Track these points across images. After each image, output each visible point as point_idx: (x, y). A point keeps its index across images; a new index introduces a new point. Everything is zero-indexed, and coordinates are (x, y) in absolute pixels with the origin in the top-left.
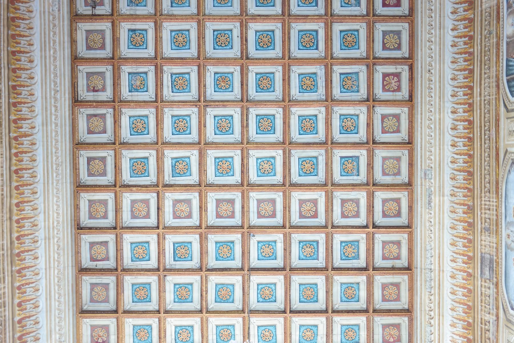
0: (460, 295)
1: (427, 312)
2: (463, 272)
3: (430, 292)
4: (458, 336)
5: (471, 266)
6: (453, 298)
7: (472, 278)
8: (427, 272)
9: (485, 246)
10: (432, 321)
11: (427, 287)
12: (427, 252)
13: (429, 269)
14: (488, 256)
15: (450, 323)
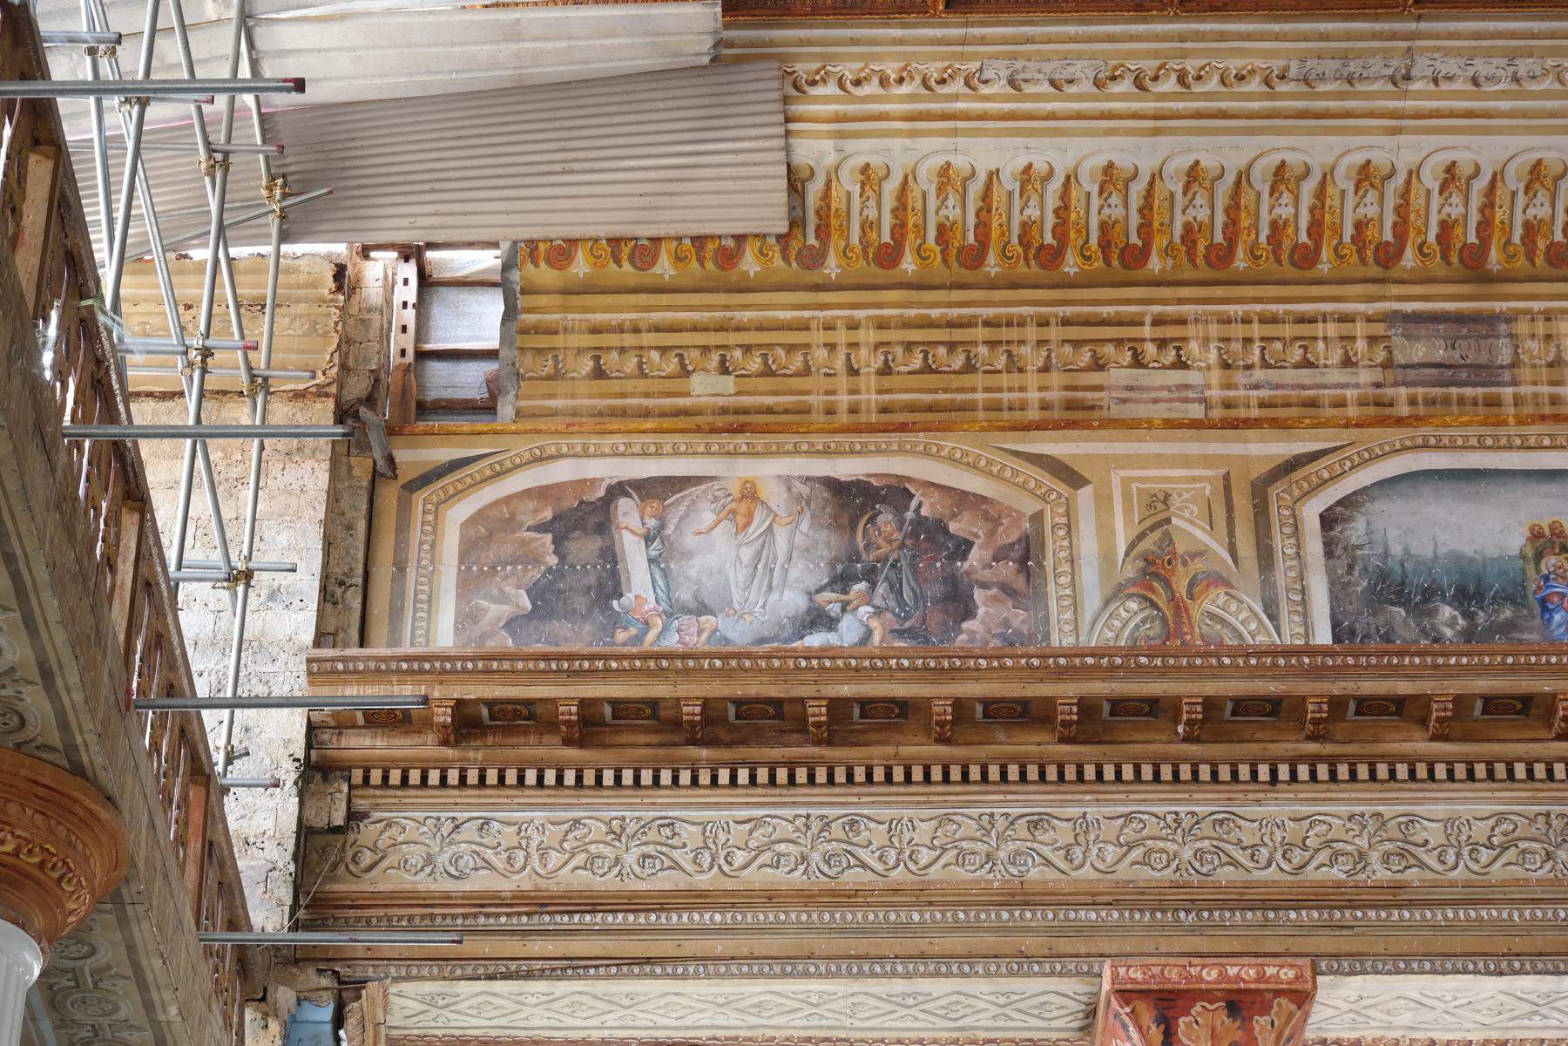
0: (1278, 211)
1: (1171, 64)
2: (1395, 225)
3: (1282, 77)
4: (1059, 203)
5: (1436, 265)
6: (1256, 173)
7: (1374, 270)
8: (1395, 63)
9: (1548, 337)
10: (1125, 86)
11: (1309, 64)
12: (1503, 62)
13: (1409, 69)
14: (1505, 356)
15: (1123, 161)
